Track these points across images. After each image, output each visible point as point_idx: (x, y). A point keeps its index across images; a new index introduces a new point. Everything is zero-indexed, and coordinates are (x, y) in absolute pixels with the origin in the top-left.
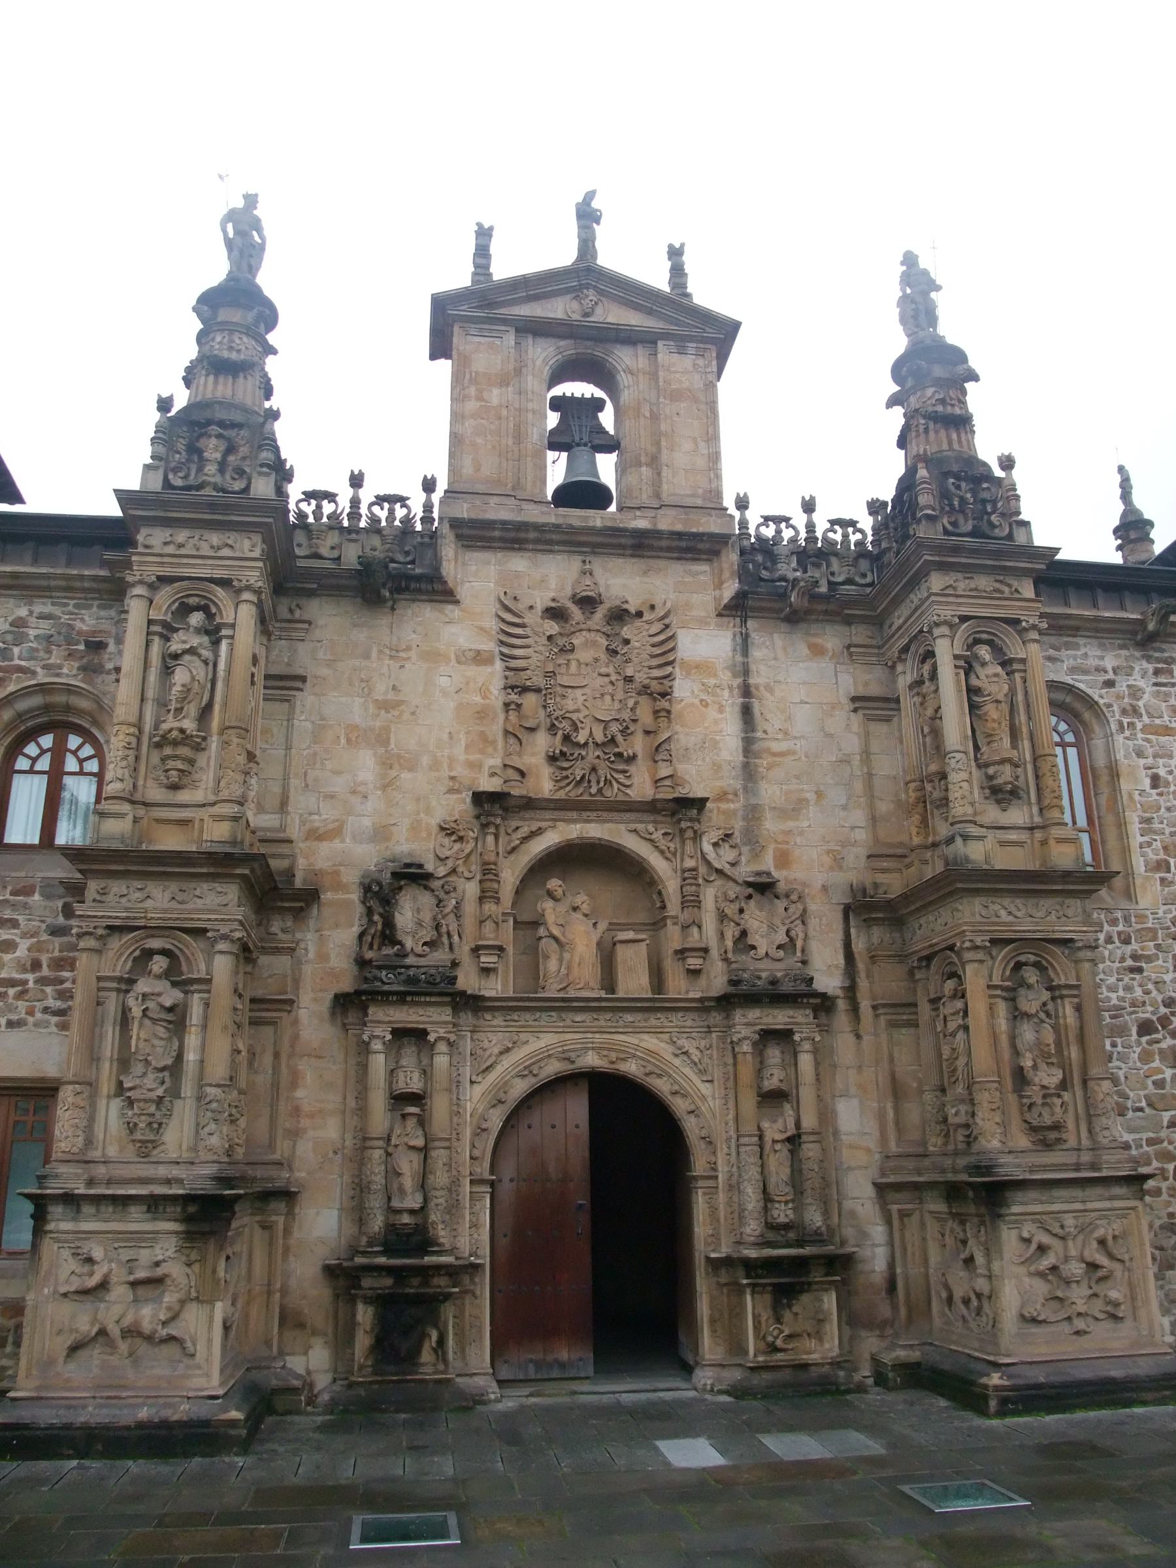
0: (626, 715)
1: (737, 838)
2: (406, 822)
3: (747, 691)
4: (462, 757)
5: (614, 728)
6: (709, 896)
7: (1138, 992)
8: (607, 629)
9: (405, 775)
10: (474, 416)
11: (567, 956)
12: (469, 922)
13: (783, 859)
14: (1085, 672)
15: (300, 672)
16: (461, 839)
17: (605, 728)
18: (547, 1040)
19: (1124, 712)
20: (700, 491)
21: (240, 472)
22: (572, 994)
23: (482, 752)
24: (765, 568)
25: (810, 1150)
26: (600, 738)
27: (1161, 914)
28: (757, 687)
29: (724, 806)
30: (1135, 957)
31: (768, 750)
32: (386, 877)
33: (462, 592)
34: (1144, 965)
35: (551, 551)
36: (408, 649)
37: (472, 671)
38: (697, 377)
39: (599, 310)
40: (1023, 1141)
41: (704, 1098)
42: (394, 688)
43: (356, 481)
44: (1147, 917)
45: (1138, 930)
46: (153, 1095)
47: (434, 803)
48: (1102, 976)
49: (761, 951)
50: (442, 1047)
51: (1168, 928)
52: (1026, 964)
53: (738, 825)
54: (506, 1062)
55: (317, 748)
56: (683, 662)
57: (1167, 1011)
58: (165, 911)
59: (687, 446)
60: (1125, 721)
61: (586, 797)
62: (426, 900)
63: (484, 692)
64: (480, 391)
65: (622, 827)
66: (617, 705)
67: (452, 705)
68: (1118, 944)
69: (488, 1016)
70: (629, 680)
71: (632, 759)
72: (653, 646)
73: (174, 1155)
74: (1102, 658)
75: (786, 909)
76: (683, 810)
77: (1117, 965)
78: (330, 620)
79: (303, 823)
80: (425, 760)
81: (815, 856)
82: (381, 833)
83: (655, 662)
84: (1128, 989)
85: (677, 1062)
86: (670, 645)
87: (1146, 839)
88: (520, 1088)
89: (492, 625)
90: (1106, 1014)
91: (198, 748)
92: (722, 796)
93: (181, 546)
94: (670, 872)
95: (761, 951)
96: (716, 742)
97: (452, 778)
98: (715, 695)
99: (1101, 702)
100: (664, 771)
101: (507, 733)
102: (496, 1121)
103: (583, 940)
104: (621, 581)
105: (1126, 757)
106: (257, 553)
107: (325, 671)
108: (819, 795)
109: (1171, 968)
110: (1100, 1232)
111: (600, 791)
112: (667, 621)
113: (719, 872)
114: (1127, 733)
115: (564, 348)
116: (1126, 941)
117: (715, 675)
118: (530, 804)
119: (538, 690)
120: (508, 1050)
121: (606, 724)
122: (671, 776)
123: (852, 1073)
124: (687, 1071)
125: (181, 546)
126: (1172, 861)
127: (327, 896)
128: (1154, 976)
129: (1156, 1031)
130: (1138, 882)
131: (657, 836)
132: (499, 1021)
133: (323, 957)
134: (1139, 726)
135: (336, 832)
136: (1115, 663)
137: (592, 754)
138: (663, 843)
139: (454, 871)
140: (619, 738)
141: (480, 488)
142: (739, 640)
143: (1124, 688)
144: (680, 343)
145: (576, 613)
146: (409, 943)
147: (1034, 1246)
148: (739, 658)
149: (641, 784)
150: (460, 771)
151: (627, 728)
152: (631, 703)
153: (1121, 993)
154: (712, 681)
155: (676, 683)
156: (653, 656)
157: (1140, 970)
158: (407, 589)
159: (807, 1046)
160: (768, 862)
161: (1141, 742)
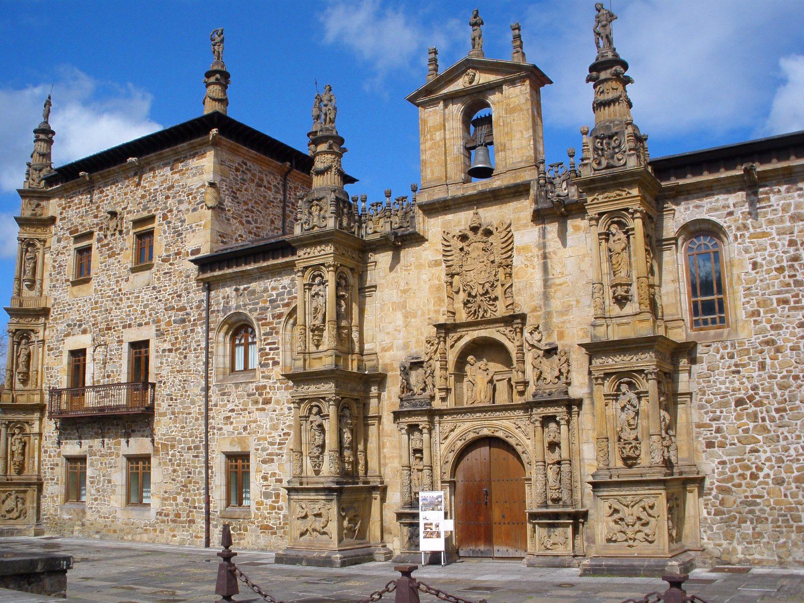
0: (492, 279)
1: (541, 328)
2: (414, 339)
3: (545, 257)
4: (432, 309)
5: (487, 286)
6: (529, 357)
7: (737, 384)
8: (485, 238)
9: (413, 320)
10: (430, 149)
11: (475, 389)
12: (437, 379)
13: (561, 335)
14: (716, 210)
15: (373, 283)
16: (433, 345)
17: (483, 287)
19: (738, 229)
20: (525, 158)
21: (324, 218)
22: (475, 405)
23: (440, 305)
24: (552, 192)
25: (565, 467)
26: (481, 291)
27: (753, 340)
28: (549, 253)
29: (535, 314)
30: (736, 365)
31: (554, 284)
32: (408, 365)
33: (429, 235)
34: (741, 369)
35: (461, 207)
36: (411, 265)
37: (434, 270)
38: (521, 97)
39: (477, 78)
40: (620, 464)
41: (528, 446)
42: (407, 283)
43: (388, 195)
44: (744, 343)
45: (739, 351)
46: (316, 455)
47: (423, 330)
48: (717, 377)
49: (548, 380)
50: (425, 431)
51: (756, 348)
52: (624, 383)
53: (541, 322)
54: (453, 434)
55: (382, 314)
56: (517, 248)
57: (753, 392)
58: (313, 392)
59: (518, 135)
60: (739, 234)
61: (479, 319)
62: (420, 371)
63: (439, 279)
64: (431, 136)
65: (494, 330)
66: (487, 275)
67: (428, 286)
68: (727, 359)
69: (445, 417)
70: (493, 262)
71: (496, 299)
72: (502, 243)
73: (326, 475)
74: (727, 199)
75: (560, 360)
76: (515, 320)
77: (726, 370)
78: (383, 259)
79: (380, 345)
80: (419, 313)
81: (575, 332)
82: (406, 346)
83: (504, 251)
84: (731, 382)
85: (517, 431)
86: (510, 241)
87: (747, 299)
88: (460, 444)
89: (441, 248)
90: (718, 396)
91: (323, 330)
92: (534, 310)
93: (309, 253)
94: (513, 348)
95: (548, 380)
96: (532, 284)
97: (429, 318)
98: (531, 261)
99: (725, 225)
100: (509, 302)
101: (448, 297)
102: (451, 457)
103: (481, 381)
104: (490, 215)
105: (738, 255)
106: (332, 251)
107: (383, 281)
108: (578, 302)
109: (757, 369)
110: (642, 504)
111: (483, 315)
112: (508, 230)
113: (533, 346)
114: (739, 240)
115: (468, 100)
116: (732, 357)
117: (531, 251)
118: (455, 327)
119: (458, 274)
120: (453, 430)
121: (483, 285)
122: (512, 304)
123: (591, 432)
124: (521, 435)
125: (309, 253)
126: (761, 310)
127: (389, 374)
128: (746, 374)
129: (746, 403)
130: (740, 324)
131: (507, 332)
132: (450, 418)
133: (390, 398)
134: (747, 235)
135: (390, 348)
136: (735, 201)
137: (479, 298)
138: (509, 335)
139: (431, 358)
140: (490, 290)
141: (433, 184)
142: (541, 231)
143: (739, 214)
144: (512, 83)
145: (470, 234)
146: (415, 390)
147: (612, 509)
148: (541, 240)
149: (501, 310)
150: (432, 315)
151: (493, 284)
152: (494, 273)
154: (530, 254)
155: (514, 259)
156: (502, 248)
157: (738, 372)
158: (406, 240)
159: (563, 422)
160: (555, 339)
161: (748, 244)
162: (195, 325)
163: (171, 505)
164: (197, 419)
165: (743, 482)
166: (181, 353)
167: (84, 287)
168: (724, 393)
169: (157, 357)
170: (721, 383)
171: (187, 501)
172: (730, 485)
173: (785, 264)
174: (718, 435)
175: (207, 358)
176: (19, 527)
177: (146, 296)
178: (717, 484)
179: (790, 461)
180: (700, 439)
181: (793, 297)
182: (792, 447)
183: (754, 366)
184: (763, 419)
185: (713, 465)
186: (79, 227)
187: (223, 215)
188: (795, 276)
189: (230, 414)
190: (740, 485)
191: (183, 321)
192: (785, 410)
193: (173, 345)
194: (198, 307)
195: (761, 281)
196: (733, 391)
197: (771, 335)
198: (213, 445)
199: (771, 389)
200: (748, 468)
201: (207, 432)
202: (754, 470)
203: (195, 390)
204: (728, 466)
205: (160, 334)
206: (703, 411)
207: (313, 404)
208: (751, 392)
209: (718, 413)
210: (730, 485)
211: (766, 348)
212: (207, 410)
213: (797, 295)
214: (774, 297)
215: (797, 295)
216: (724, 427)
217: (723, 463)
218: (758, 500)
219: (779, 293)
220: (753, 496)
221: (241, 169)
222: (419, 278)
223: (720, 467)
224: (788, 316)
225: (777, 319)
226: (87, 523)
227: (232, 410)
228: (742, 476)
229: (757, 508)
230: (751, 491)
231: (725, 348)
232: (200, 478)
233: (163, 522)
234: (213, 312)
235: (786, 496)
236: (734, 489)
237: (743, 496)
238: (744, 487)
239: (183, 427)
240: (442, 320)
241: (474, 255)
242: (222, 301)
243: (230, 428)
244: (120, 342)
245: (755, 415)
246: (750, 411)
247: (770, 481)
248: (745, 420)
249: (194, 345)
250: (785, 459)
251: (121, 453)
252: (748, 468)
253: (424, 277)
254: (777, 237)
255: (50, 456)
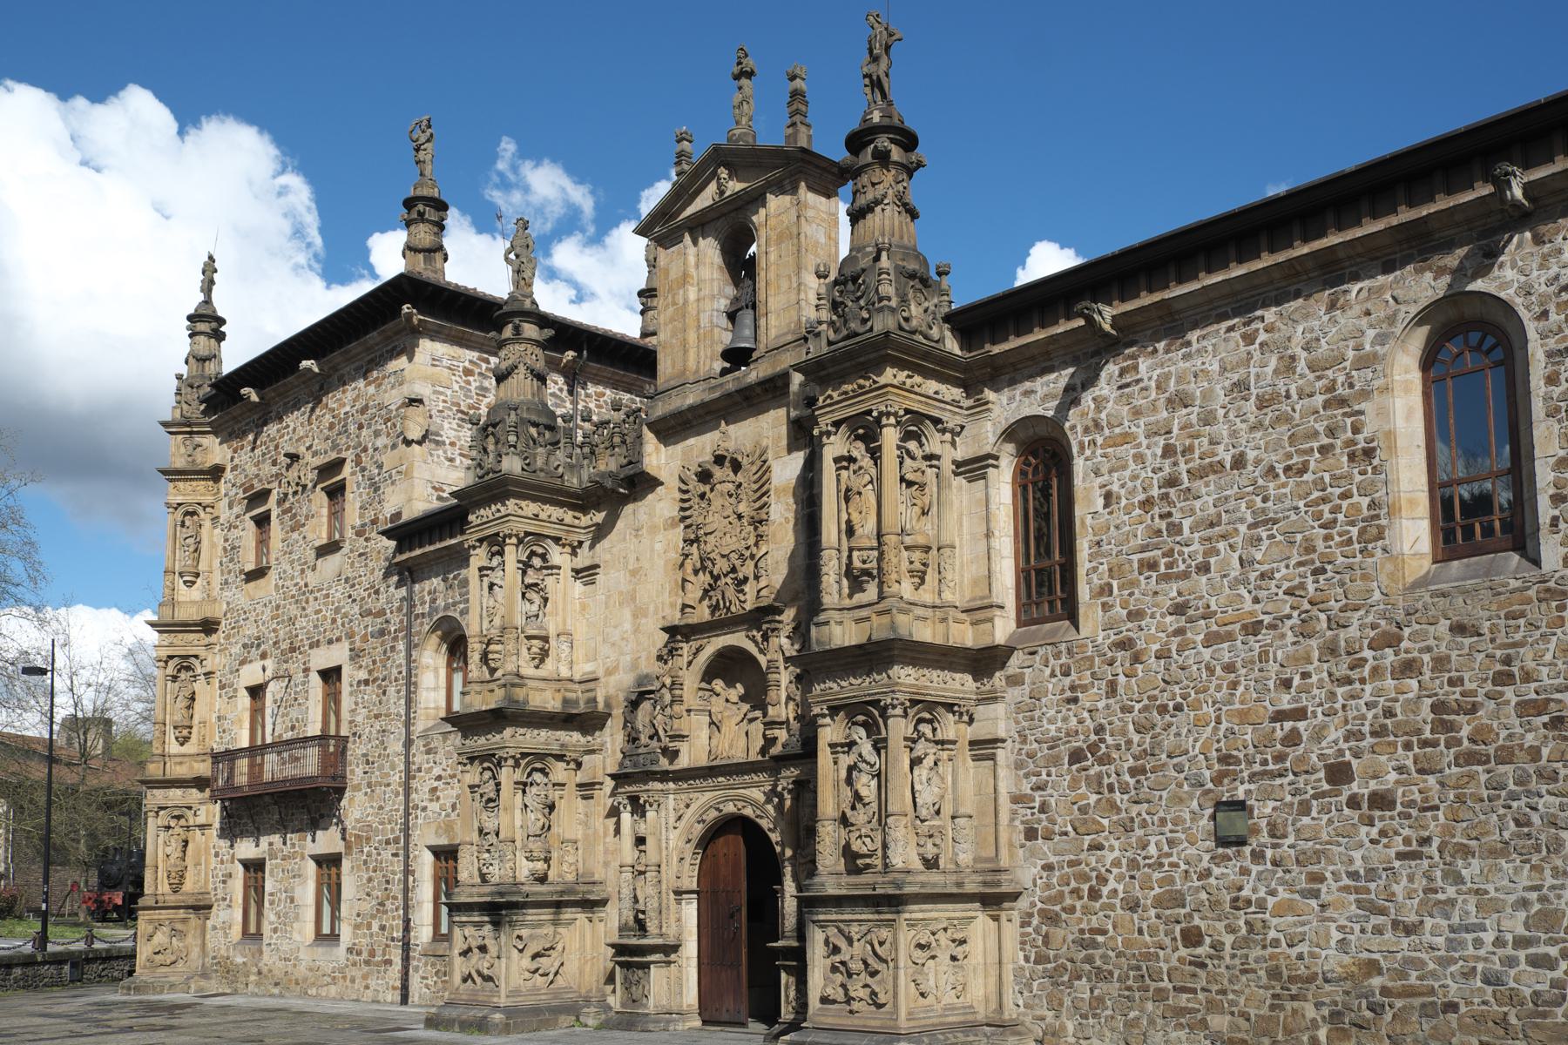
7: (1074, 721)
18: (709, 795)
27: (1100, 639)
80: (652, 608)
82: (634, 665)
84: (1065, 719)
88: (699, 829)
116: (1066, 674)
126: (1115, 584)
128: (1088, 705)
129: (1086, 759)
135: (616, 668)
153: (1059, 724)
157: (1075, 700)
162: (395, 639)
163: (365, 935)
164: (397, 794)
165: (1078, 905)
166: (379, 687)
167: (261, 582)
168: (1054, 739)
169: (351, 694)
170: (1050, 722)
171: (383, 928)
172: (1057, 908)
173: (1155, 492)
174: (1043, 816)
175: (409, 692)
176: (171, 979)
177: (338, 592)
178: (1040, 905)
179: (1149, 866)
180: (1017, 823)
181: (1164, 555)
182: (1153, 839)
183: (1100, 688)
184: (1111, 789)
185: (1035, 871)
186: (255, 482)
187: (441, 452)
188: (1170, 514)
189: (436, 784)
190: (1072, 910)
191: (382, 633)
192: (1143, 771)
193: (370, 672)
194: (400, 609)
195: (1117, 527)
196: (1068, 735)
197: (1128, 629)
198: (416, 835)
199: (1124, 733)
200: (1084, 878)
201: (407, 814)
202: (1094, 882)
203: (397, 747)
204: (1057, 873)
205: (356, 655)
206: (1021, 773)
207: (486, 765)
208: (1093, 737)
209: (1044, 776)
210: (1057, 908)
211: (1120, 655)
212: (409, 776)
213: (1170, 553)
214: (1135, 558)
215: (1170, 553)
216: (1053, 801)
217: (1048, 868)
218: (1100, 939)
219: (1143, 549)
220: (1091, 931)
221: (477, 371)
222: (652, 550)
223: (1045, 874)
224: (1156, 593)
225: (1139, 599)
226: (265, 970)
227: (439, 778)
228: (1076, 892)
229: (1097, 953)
230: (1089, 921)
231: (1057, 656)
232: (397, 889)
233: (354, 964)
234: (417, 616)
235: (1140, 932)
236: (1064, 916)
237: (1076, 929)
238: (1078, 914)
239: (381, 808)
240: (676, 618)
241: (717, 503)
242: (427, 598)
243: (434, 806)
244: (306, 670)
245: (1099, 776)
246: (1092, 772)
247: (1117, 902)
248: (1083, 790)
249: (395, 671)
250: (1142, 863)
251: (307, 853)
252: (1087, 878)
253: (658, 546)
254: (1145, 442)
255: (222, 862)
